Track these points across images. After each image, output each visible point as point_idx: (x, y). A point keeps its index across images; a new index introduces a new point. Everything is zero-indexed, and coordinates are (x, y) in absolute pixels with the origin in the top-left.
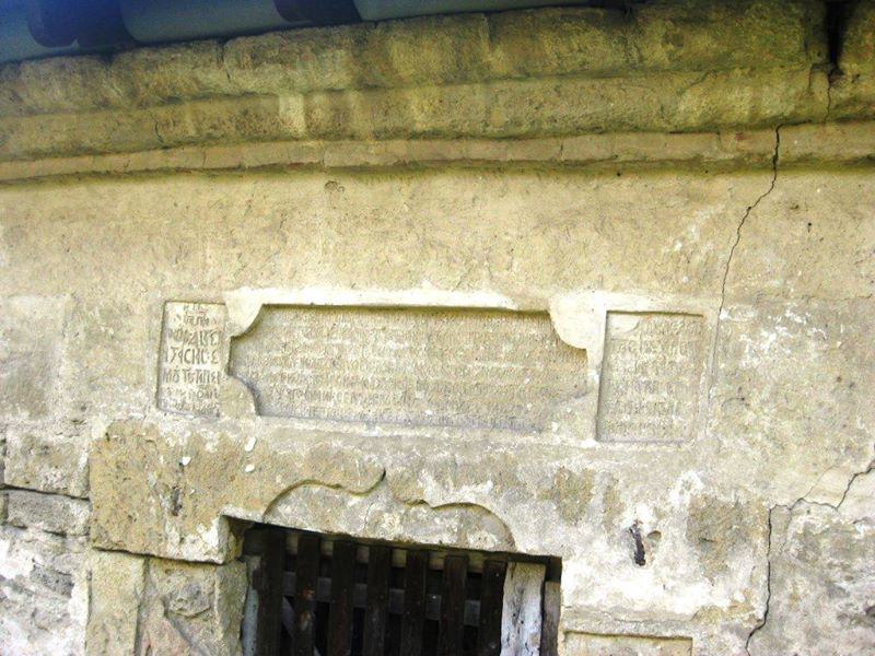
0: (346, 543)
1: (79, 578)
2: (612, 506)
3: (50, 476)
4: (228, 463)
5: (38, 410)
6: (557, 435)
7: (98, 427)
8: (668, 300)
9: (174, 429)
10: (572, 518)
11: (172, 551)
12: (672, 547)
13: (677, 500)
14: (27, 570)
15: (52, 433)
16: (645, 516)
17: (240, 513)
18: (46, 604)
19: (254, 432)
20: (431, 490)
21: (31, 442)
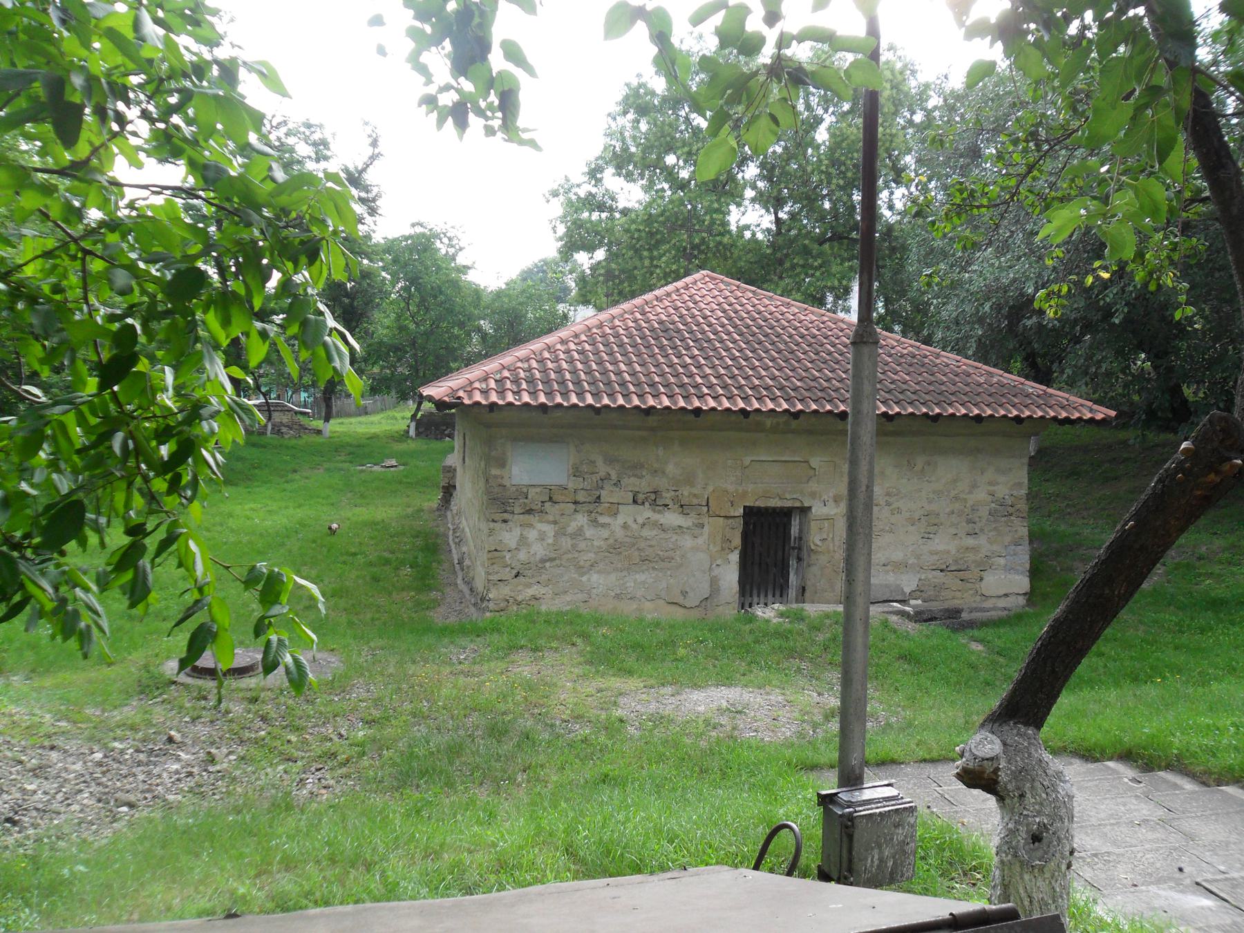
0: (774, 509)
1: (706, 523)
2: (820, 497)
3: (695, 501)
4: (745, 494)
5: (692, 485)
6: (811, 484)
7: (710, 489)
8: (830, 459)
9: (731, 488)
10: (814, 499)
11: (732, 514)
12: (831, 503)
13: (831, 494)
14: (691, 524)
15: (695, 491)
16: (825, 497)
17: (748, 504)
18: (697, 531)
19: (750, 487)
20: (788, 496)
21: (690, 494)
